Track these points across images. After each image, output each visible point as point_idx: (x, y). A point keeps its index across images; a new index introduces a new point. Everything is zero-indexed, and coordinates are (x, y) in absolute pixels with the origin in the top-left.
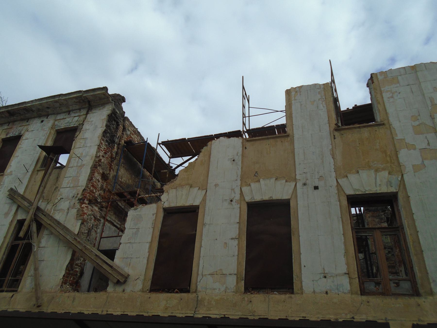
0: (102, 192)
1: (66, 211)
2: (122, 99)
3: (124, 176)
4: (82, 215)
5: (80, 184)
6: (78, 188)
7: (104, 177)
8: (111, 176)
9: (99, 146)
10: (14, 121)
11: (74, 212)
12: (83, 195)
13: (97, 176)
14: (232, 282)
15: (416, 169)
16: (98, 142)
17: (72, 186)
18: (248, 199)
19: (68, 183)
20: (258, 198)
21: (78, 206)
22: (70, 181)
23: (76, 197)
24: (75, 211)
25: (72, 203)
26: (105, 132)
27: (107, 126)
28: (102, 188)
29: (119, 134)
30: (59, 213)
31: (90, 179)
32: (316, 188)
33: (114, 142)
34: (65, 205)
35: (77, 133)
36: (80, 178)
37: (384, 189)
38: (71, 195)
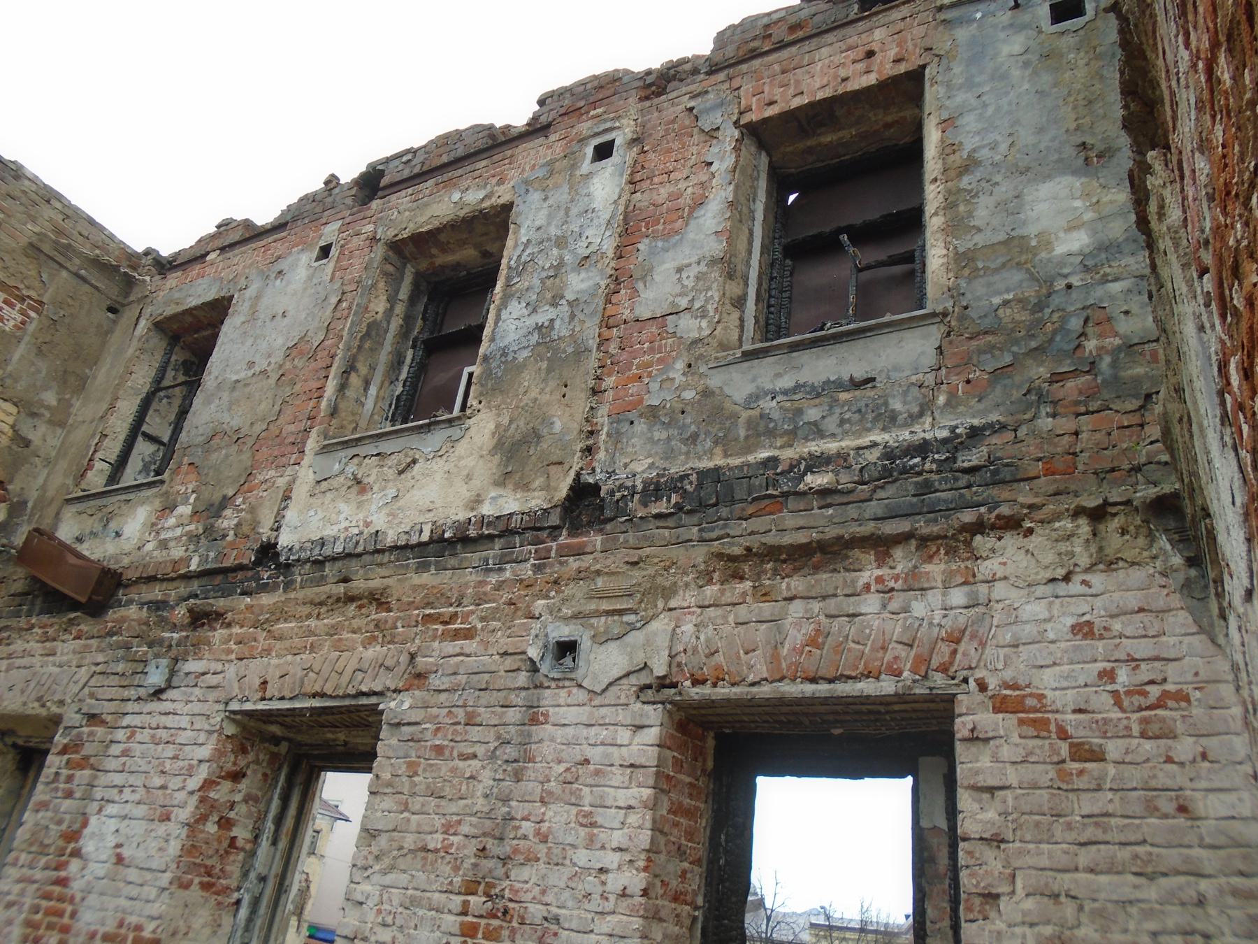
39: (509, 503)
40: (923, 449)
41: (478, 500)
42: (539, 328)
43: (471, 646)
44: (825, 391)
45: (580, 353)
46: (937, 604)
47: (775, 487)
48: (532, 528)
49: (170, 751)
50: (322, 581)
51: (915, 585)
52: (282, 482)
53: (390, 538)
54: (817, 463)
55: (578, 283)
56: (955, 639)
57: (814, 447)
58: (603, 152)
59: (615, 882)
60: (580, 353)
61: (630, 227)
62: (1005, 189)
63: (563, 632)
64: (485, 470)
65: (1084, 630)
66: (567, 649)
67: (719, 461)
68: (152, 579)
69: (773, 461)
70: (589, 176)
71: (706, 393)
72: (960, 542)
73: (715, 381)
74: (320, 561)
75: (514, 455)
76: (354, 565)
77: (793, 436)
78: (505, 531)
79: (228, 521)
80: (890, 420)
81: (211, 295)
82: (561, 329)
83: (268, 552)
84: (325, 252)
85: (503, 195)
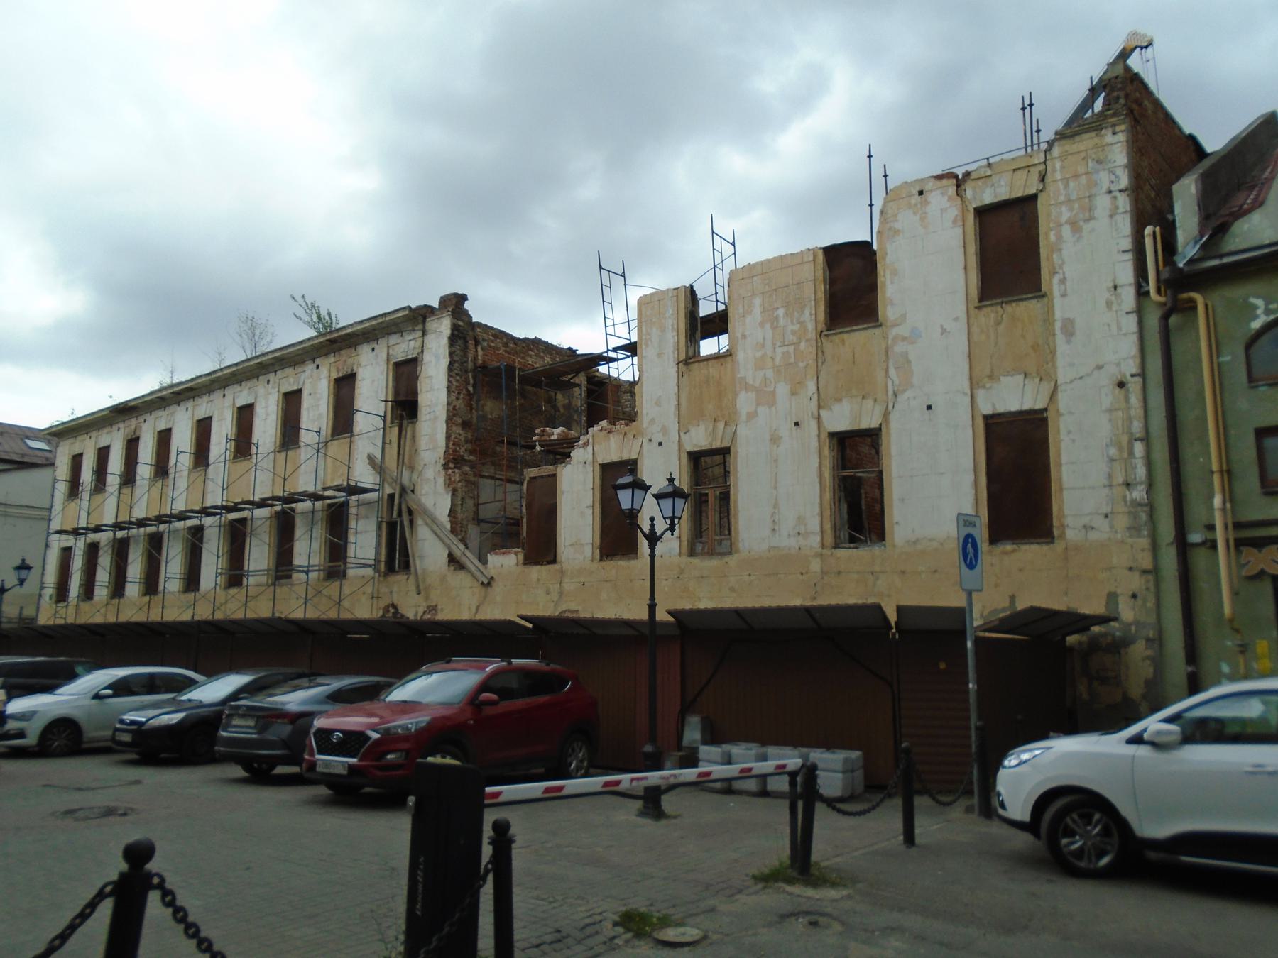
0: (469, 446)
2: (462, 298)
3: (492, 408)
7: (466, 425)
8: (475, 420)
9: (449, 389)
10: (340, 349)
11: (441, 480)
13: (458, 430)
14: (588, 551)
15: (752, 416)
16: (445, 383)
18: (600, 460)
20: (608, 460)
26: (451, 364)
27: (451, 354)
28: (467, 441)
29: (470, 357)
31: (448, 437)
32: (660, 444)
33: (466, 371)
37: (717, 444)
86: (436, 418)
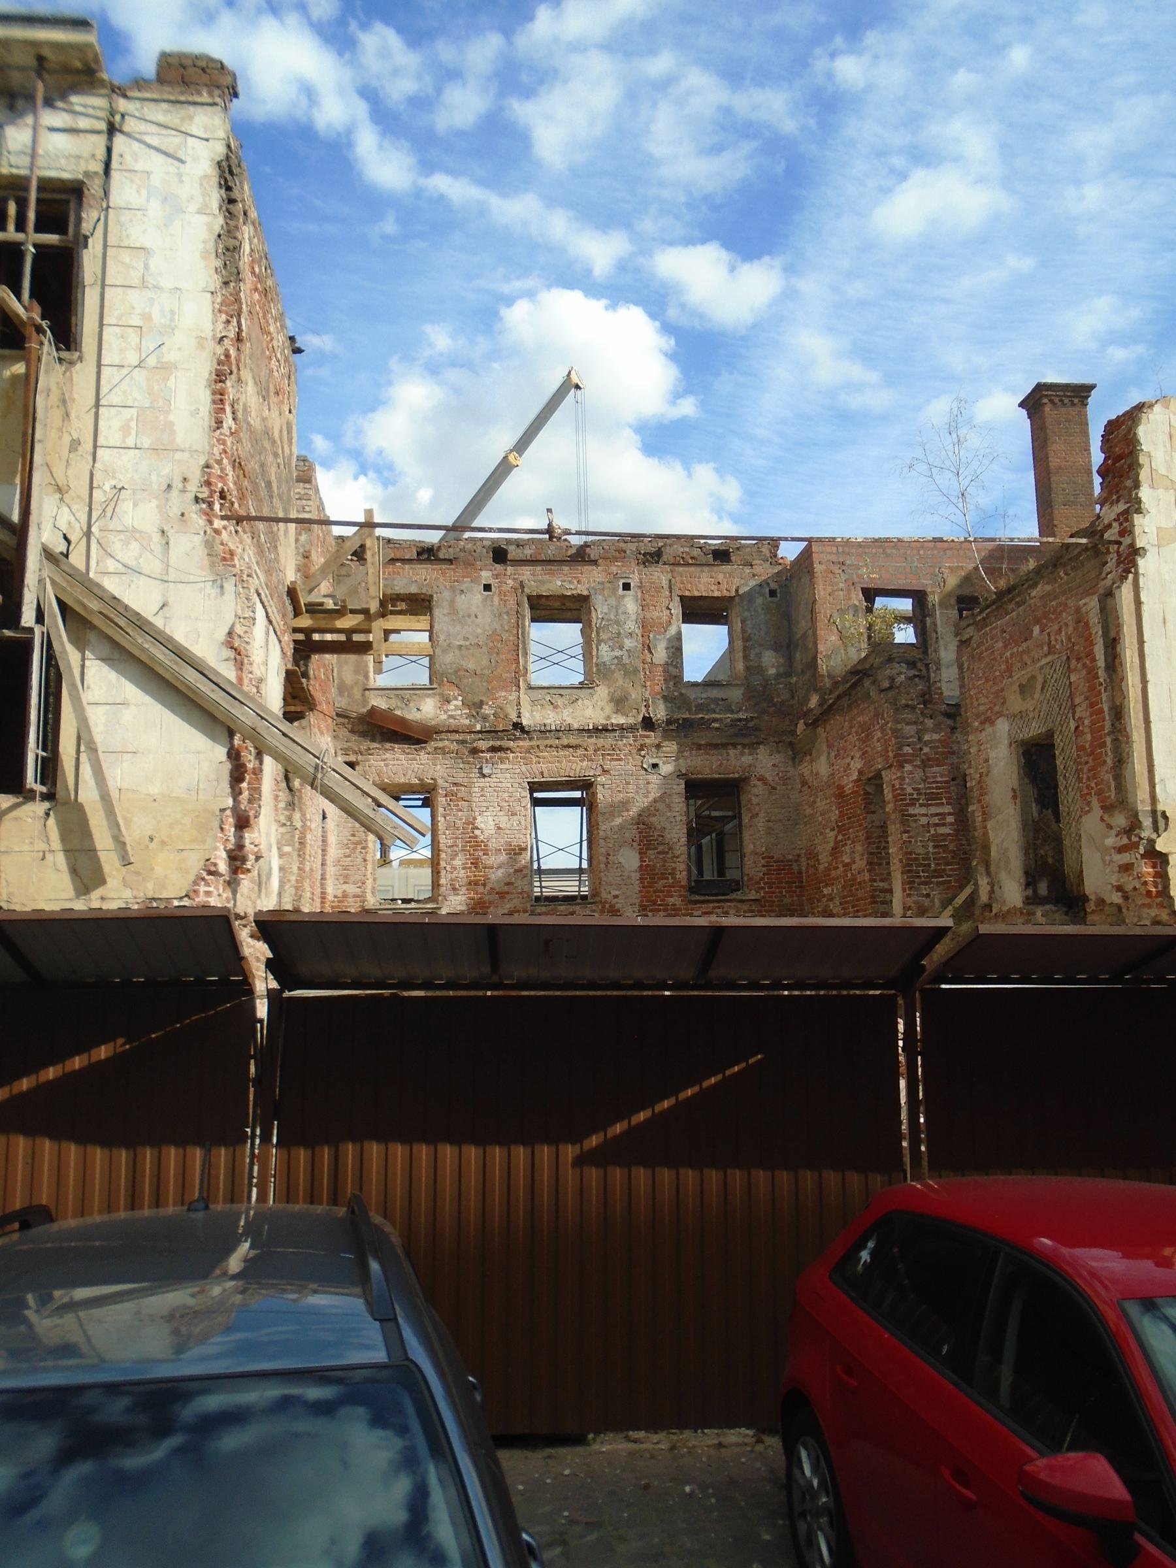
1: (157, 537)
4: (224, 559)
5: (180, 439)
6: (178, 456)
12: (208, 483)
17: (146, 442)
19: (125, 429)
21: (201, 522)
22: (133, 424)
23: (184, 491)
24: (198, 540)
25: (175, 511)
30: (127, 543)
34: (140, 514)
35: (90, 216)
36: (171, 418)
38: (157, 482)
39: (621, 720)
40: (740, 720)
41: (608, 718)
42: (616, 657)
43: (622, 763)
44: (716, 701)
45: (636, 671)
46: (747, 759)
47: (704, 724)
48: (632, 728)
49: (506, 795)
50: (547, 738)
51: (742, 754)
52: (513, 697)
53: (576, 726)
54: (715, 720)
55: (628, 643)
56: (750, 766)
57: (714, 716)
58: (627, 587)
59: (678, 819)
60: (636, 671)
61: (646, 626)
62: (757, 650)
63: (655, 761)
64: (609, 708)
65: (774, 765)
66: (655, 766)
67: (687, 716)
68: (457, 732)
69: (703, 718)
70: (623, 596)
71: (681, 694)
72: (753, 747)
73: (683, 691)
74: (544, 732)
75: (619, 702)
76: (561, 734)
77: (708, 711)
78: (622, 728)
79: (487, 710)
80: (732, 712)
81: (414, 589)
82: (626, 660)
83: (518, 726)
84: (487, 588)
85: (582, 590)
86: (165, 369)
